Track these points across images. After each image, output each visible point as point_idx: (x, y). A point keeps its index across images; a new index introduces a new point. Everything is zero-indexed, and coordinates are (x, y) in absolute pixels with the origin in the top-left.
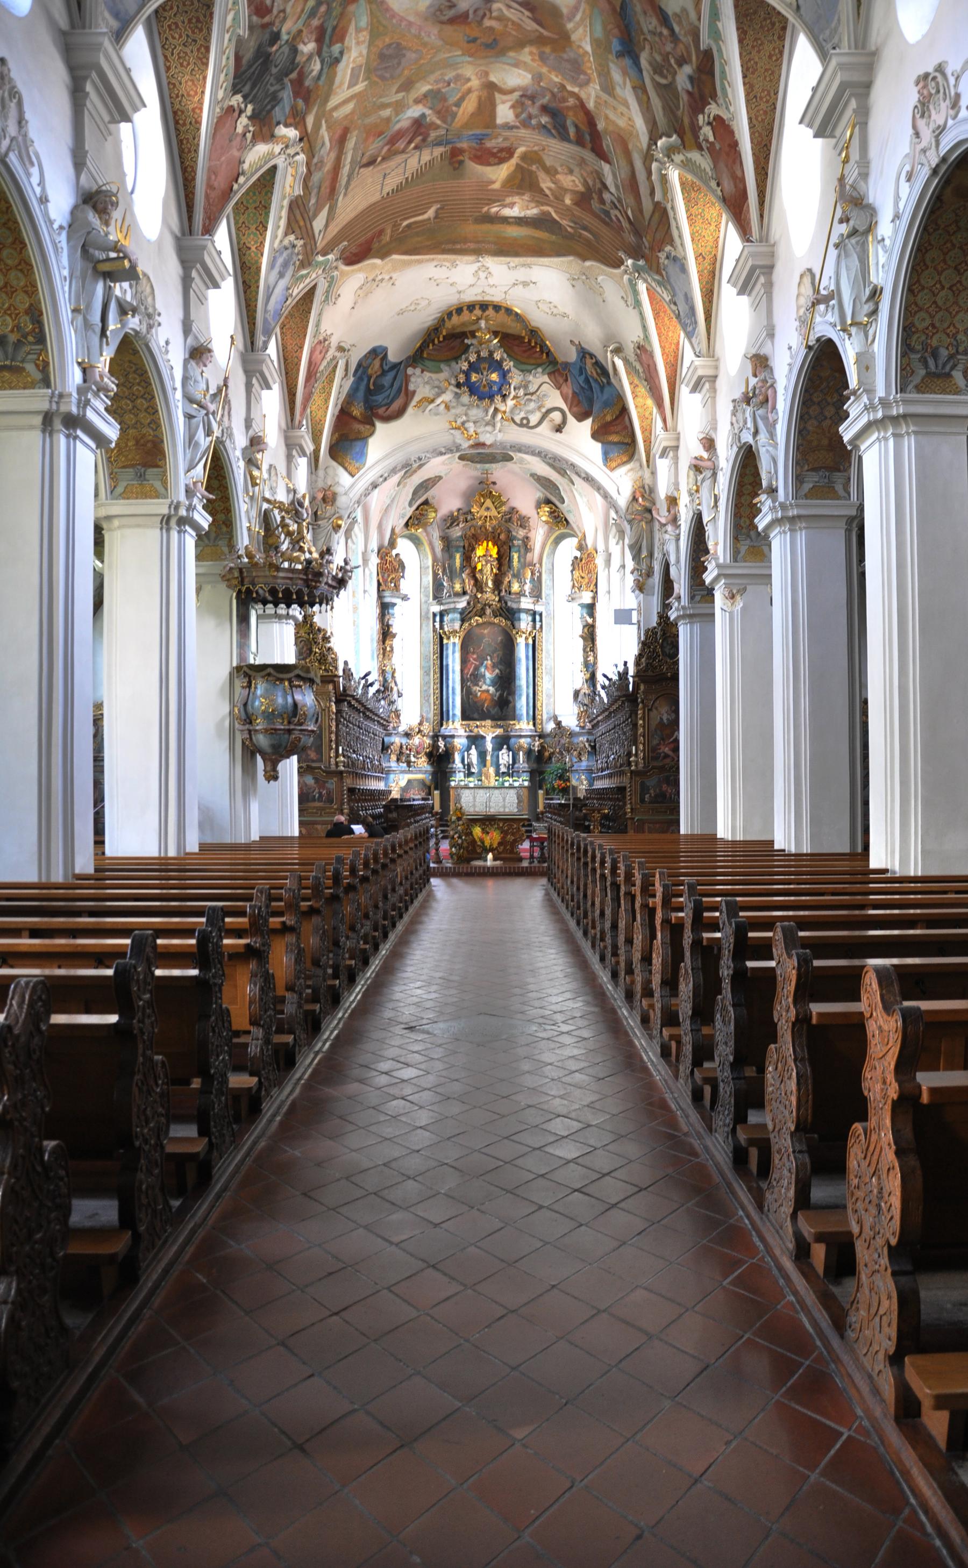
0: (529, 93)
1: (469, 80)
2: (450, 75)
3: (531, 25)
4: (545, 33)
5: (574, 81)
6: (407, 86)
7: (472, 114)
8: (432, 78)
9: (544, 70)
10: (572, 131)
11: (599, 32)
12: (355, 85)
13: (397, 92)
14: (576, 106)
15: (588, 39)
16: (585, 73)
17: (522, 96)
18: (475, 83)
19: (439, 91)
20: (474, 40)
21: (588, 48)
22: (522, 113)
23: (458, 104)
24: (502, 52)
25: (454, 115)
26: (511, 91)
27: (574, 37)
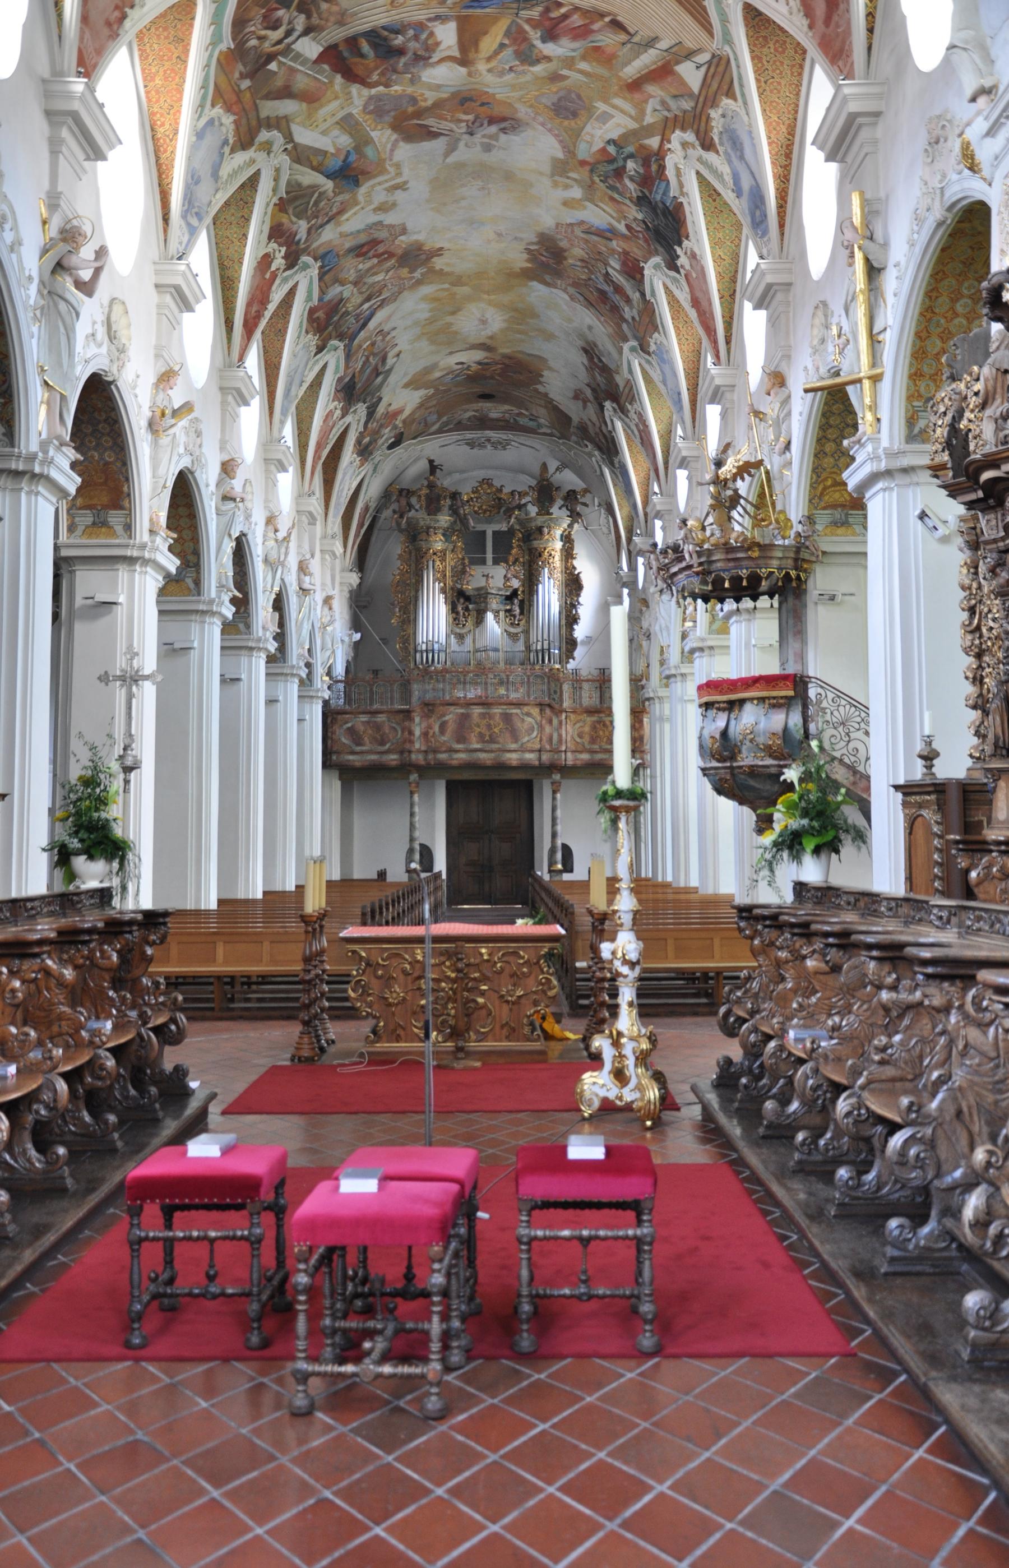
0: (421, 63)
1: (489, 71)
2: (509, 77)
3: (430, 122)
4: (416, 121)
5: (378, 98)
6: (555, 78)
7: (485, 33)
8: (528, 77)
9: (410, 90)
10: (365, 47)
11: (369, 151)
12: (605, 112)
13: (565, 78)
14: (368, 76)
15: (376, 139)
16: (370, 113)
17: (430, 58)
18: (482, 67)
19: (523, 62)
20: (483, 104)
21: (373, 134)
22: (427, 39)
23: (502, 46)
24: (454, 95)
25: (507, 34)
26: (442, 60)
27: (389, 131)
